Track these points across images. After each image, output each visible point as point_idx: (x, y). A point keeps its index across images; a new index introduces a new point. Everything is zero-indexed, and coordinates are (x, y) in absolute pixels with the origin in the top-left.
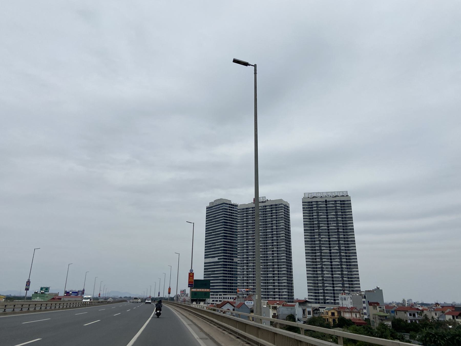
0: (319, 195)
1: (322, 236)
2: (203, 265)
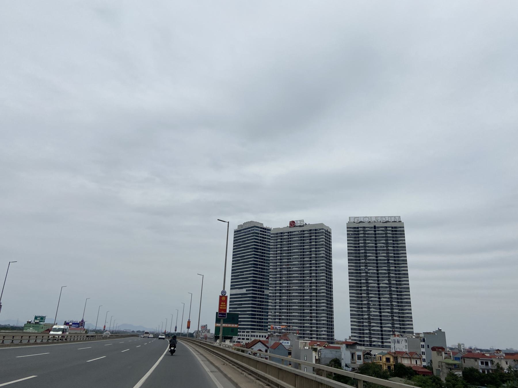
0: (367, 219)
1: (369, 268)
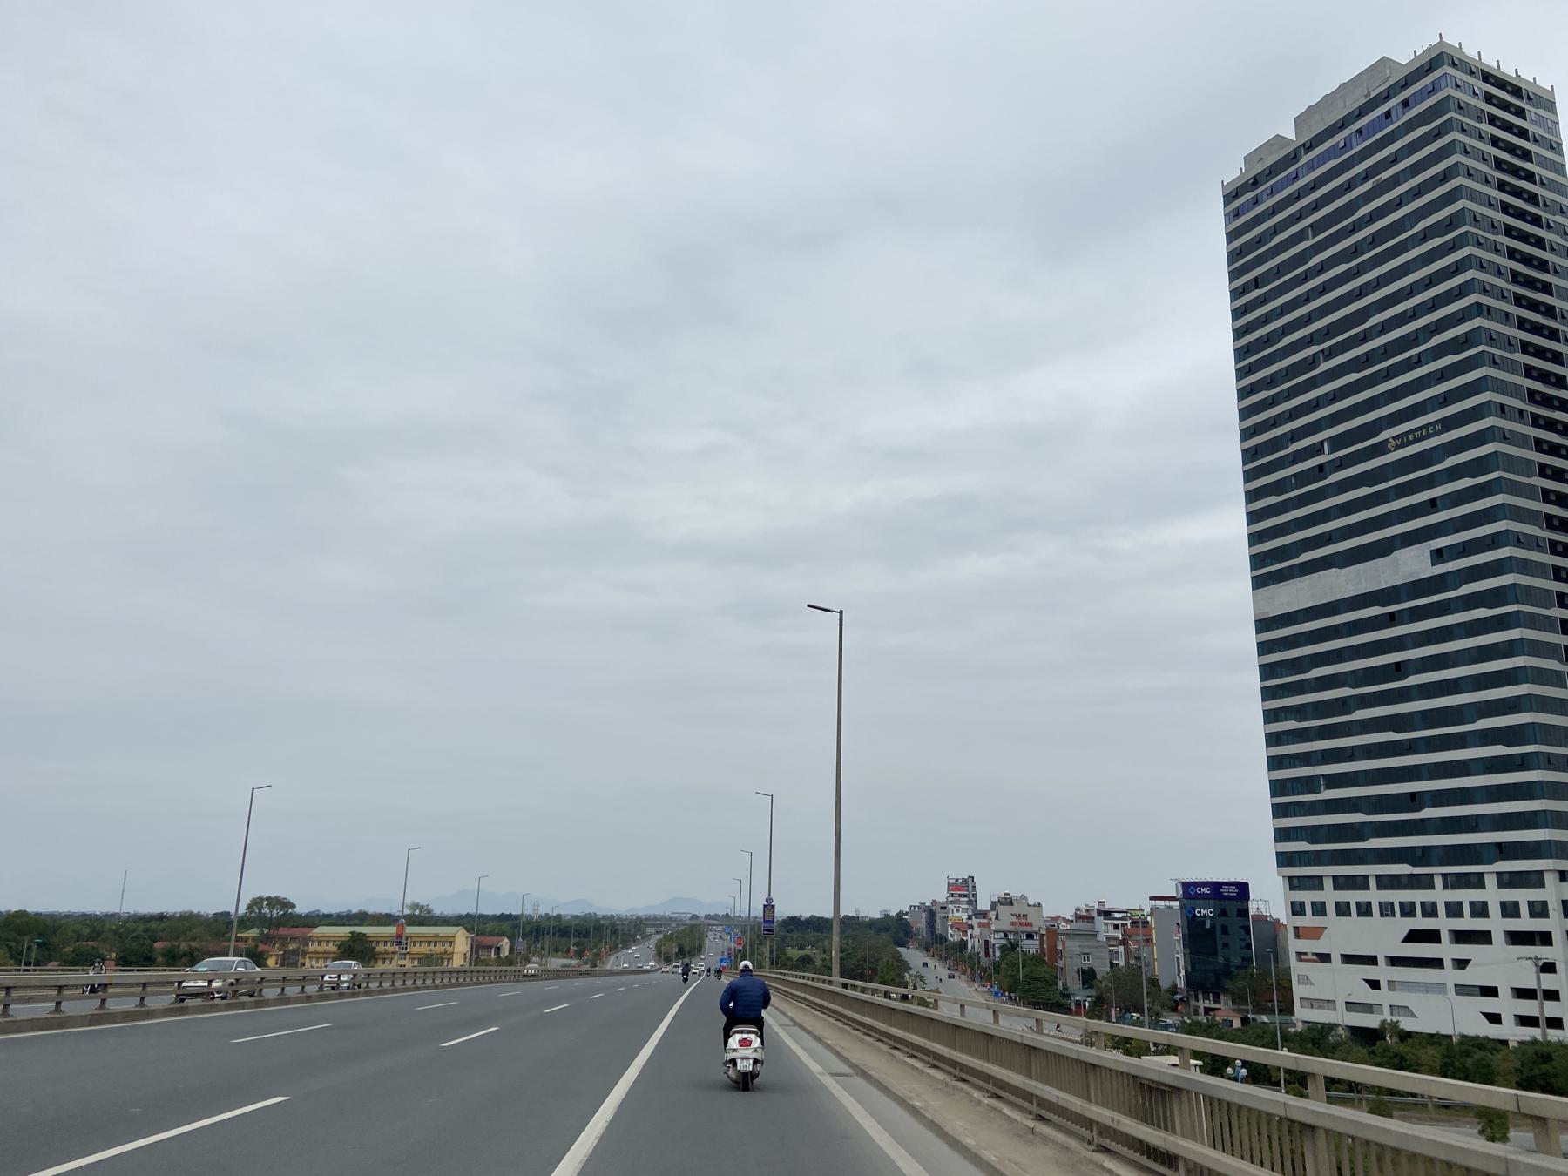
2: (1248, 639)
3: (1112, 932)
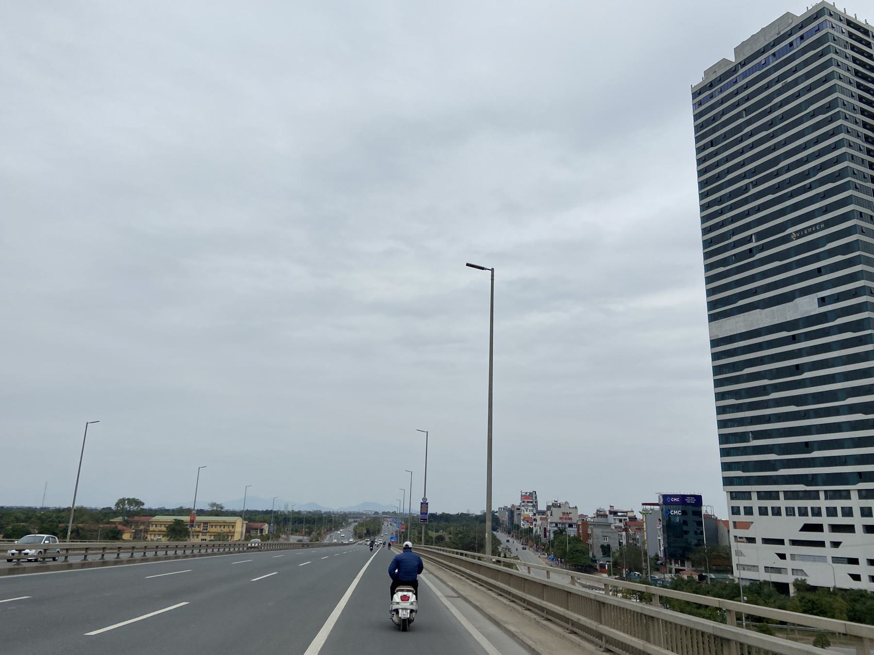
2: (707, 352)
3: (618, 524)
